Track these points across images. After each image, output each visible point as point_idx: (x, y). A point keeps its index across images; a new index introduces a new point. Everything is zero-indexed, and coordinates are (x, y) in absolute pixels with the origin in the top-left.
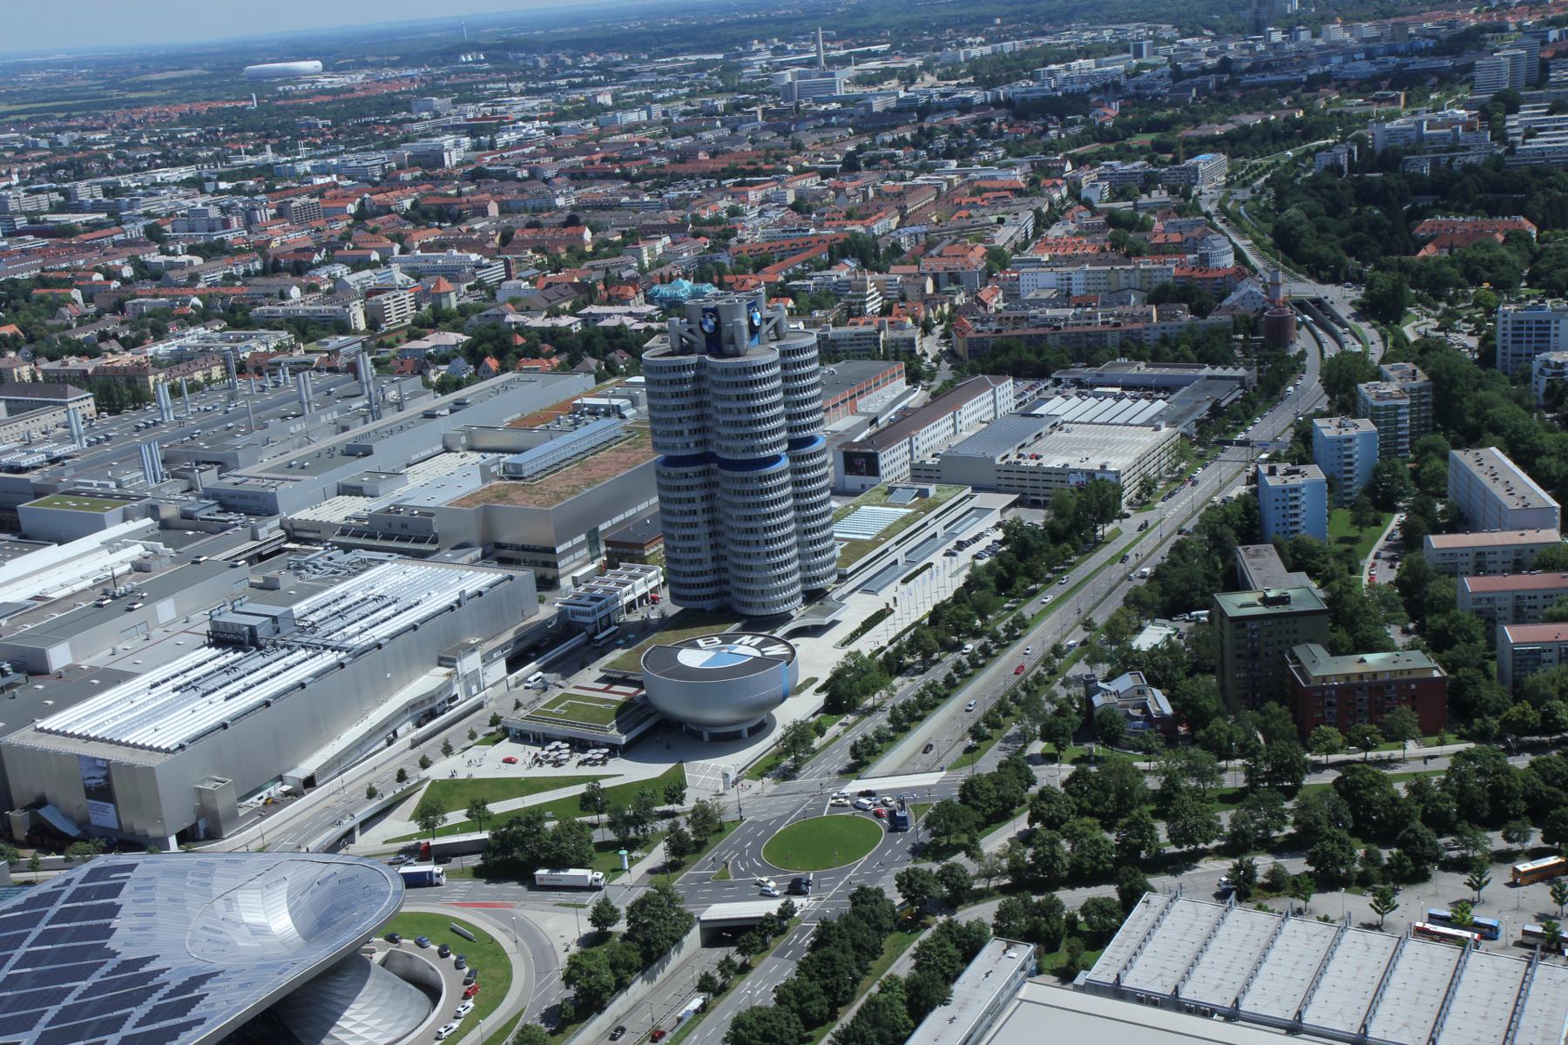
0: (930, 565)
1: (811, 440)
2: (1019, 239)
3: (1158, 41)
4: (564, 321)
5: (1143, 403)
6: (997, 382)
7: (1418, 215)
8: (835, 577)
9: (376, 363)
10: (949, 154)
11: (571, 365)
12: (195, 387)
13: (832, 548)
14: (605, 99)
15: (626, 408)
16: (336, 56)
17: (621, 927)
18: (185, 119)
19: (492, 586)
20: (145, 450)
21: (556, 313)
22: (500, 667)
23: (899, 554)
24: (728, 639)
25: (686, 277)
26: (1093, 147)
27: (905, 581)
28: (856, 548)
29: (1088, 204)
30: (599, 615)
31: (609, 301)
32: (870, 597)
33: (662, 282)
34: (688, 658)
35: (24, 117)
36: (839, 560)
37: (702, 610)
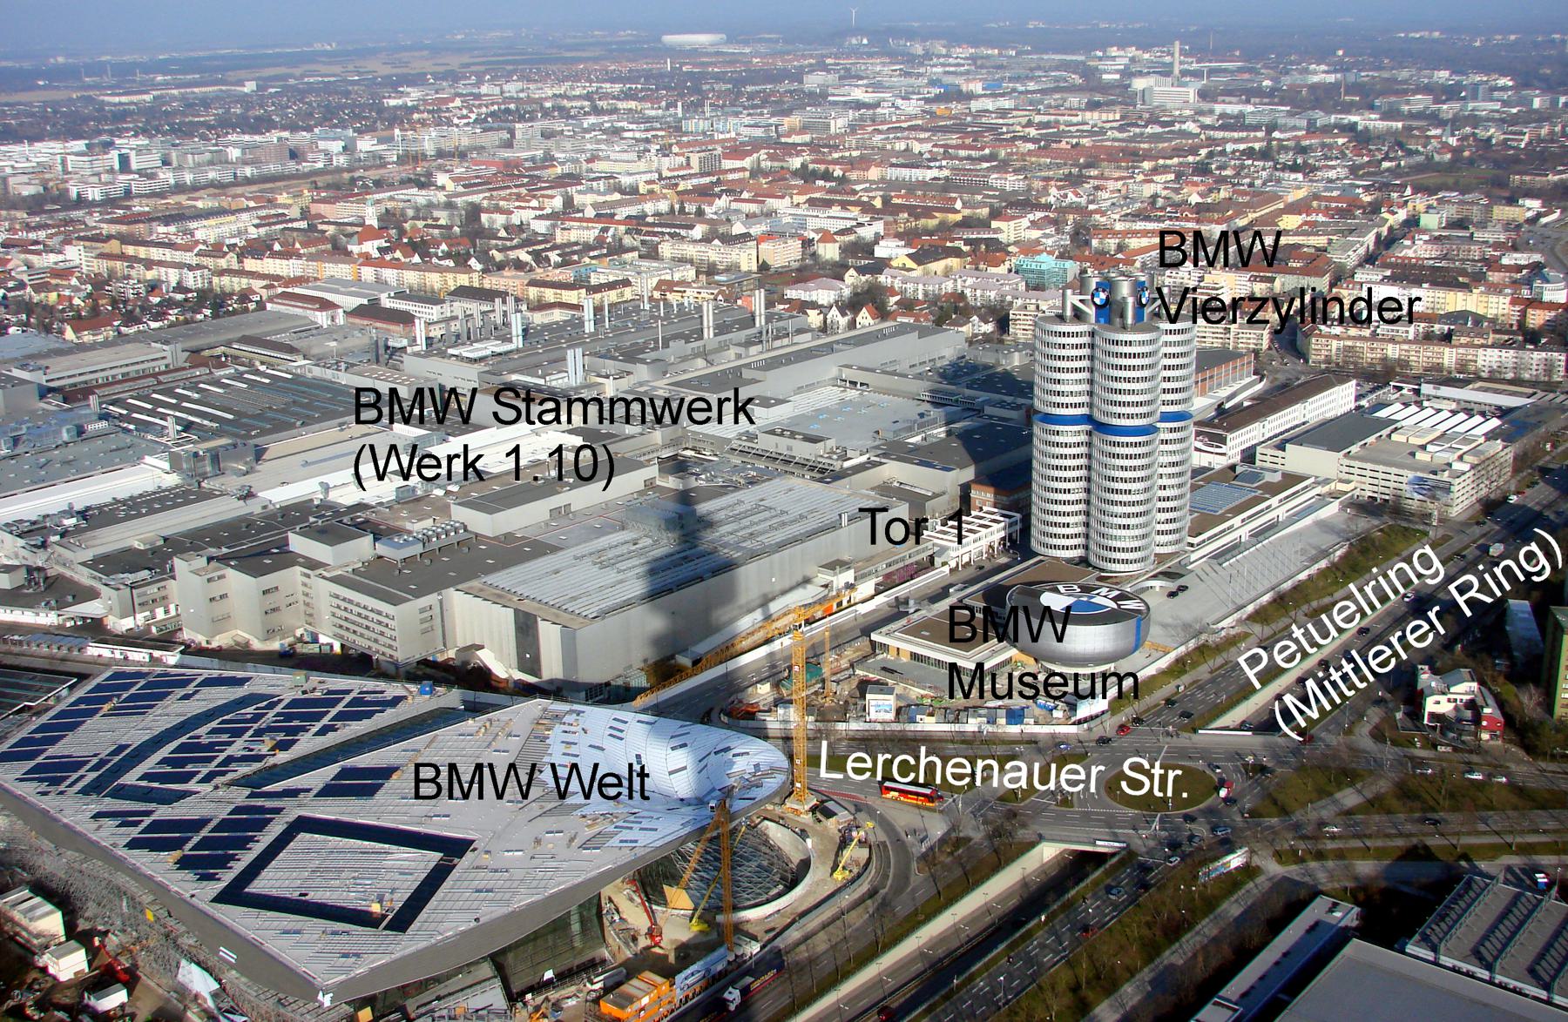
5: (1478, 419)
10: (1295, 168)
14: (977, 87)
20: (570, 353)
35: (482, 68)
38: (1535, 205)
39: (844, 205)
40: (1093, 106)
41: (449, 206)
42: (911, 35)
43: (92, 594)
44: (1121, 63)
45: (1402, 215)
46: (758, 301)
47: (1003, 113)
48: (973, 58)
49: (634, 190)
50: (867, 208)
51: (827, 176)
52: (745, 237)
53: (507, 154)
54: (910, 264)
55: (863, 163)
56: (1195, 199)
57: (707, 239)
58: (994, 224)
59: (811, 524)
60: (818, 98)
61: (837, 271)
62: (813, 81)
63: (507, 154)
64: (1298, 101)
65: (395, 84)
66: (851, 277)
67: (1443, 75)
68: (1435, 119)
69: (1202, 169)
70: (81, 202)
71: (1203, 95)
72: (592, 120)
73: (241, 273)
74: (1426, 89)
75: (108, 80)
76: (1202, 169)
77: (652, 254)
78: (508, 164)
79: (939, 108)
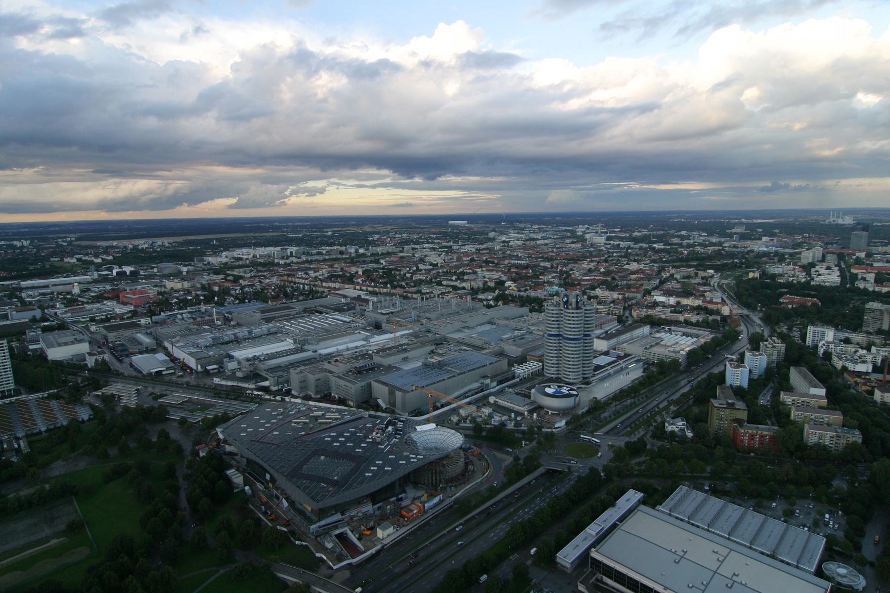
1: (589, 335)
3: (700, 236)
4: (522, 294)
7: (782, 295)
9: (473, 299)
10: (635, 261)
11: (522, 306)
12: (427, 299)
16: (471, 219)
17: (521, 462)
18: (433, 233)
21: (520, 291)
22: (495, 384)
23: (611, 371)
24: (559, 387)
26: (678, 264)
28: (598, 368)
29: (676, 279)
34: (548, 390)
38: (712, 271)
39: (497, 271)
40: (573, 243)
41: (383, 269)
42: (521, 222)
43: (267, 379)
44: (583, 230)
45: (668, 275)
46: (469, 298)
47: (546, 245)
48: (539, 229)
49: (437, 265)
50: (503, 272)
51: (493, 262)
52: (467, 280)
53: (401, 254)
55: (504, 258)
56: (602, 270)
57: (456, 280)
59: (478, 365)
60: (493, 240)
61: (492, 290)
62: (491, 235)
63: (401, 254)
64: (636, 240)
65: (371, 234)
66: (497, 292)
67: (683, 233)
68: (681, 246)
69: (606, 261)
70: (278, 264)
71: (608, 239)
72: (426, 245)
73: (322, 286)
74: (678, 236)
75: (289, 230)
76: (606, 261)
77: (439, 284)
78: (402, 257)
79: (528, 243)
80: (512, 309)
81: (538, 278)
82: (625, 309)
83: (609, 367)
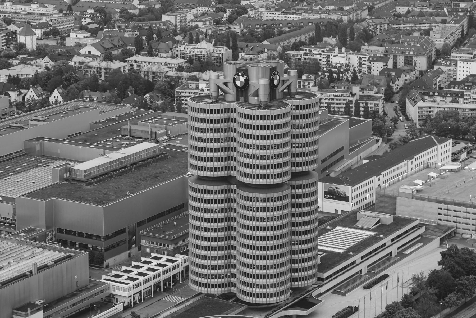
0: (386, 276)
2: (457, 35)
4: (116, 65)
6: (440, 142)
8: (314, 280)
13: (315, 257)
15: (162, 135)
19: (57, 262)
23: (364, 267)
25: (209, 41)
27: (368, 287)
30: (133, 292)
31: (150, 54)
32: (340, 297)
33: (191, 42)
36: (319, 265)
37: (213, 295)
54: (95, 52)
58: (165, 18)
80: (95, 110)
81: (159, 18)
82: (389, 97)
83: (357, 258)
